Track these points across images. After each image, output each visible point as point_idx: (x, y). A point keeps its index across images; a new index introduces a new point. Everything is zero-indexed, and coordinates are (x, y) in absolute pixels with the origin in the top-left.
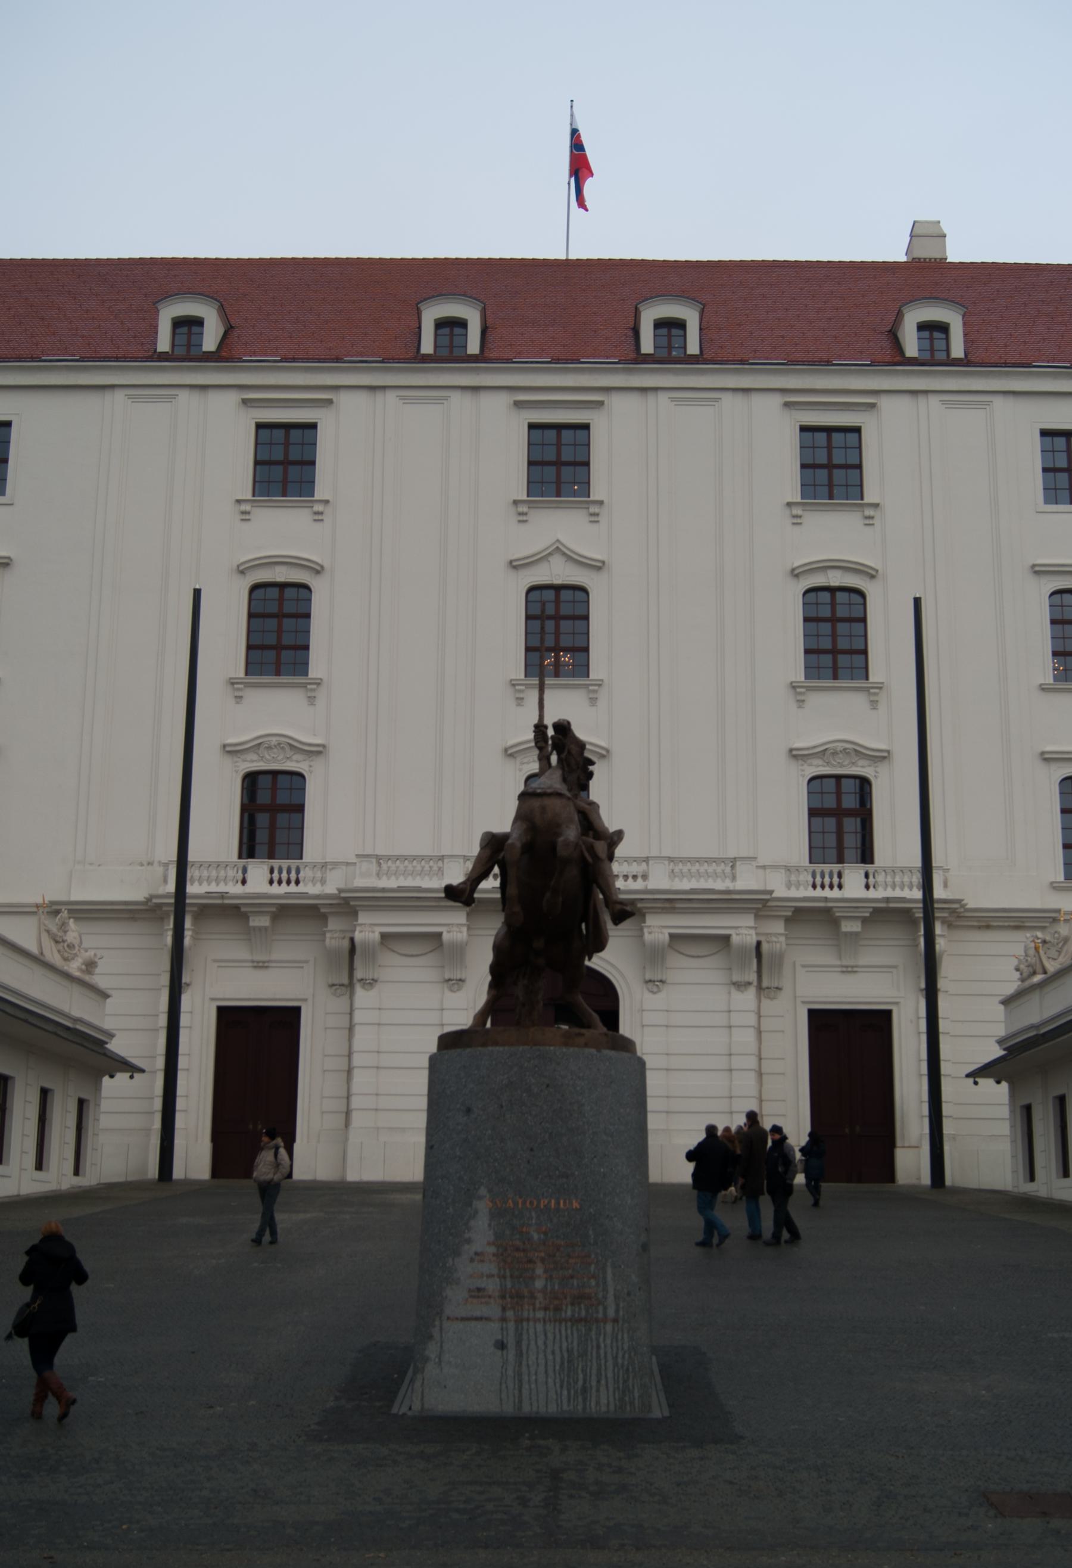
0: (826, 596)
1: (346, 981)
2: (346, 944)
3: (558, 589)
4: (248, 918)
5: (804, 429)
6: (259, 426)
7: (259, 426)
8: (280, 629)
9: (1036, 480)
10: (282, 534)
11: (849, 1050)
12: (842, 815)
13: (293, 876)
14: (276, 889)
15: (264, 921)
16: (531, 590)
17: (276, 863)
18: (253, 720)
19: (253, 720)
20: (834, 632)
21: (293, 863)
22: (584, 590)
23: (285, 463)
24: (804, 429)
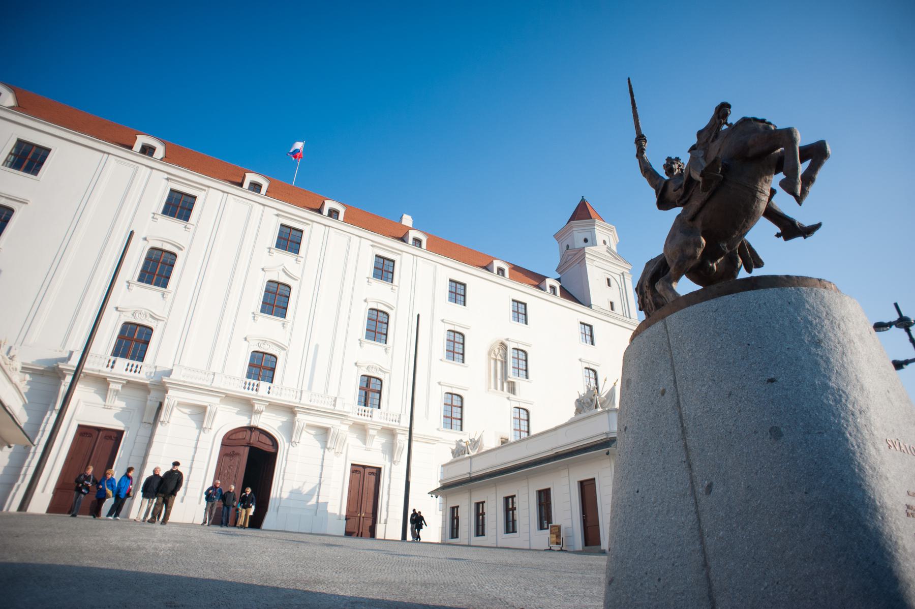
0: (375, 313)
1: (152, 422)
2: (157, 405)
3: (278, 283)
4: (109, 384)
5: (377, 256)
6: (172, 191)
7: (172, 191)
8: (158, 268)
9: (447, 294)
10: (169, 233)
11: (365, 483)
12: (370, 390)
13: (138, 369)
14: (128, 373)
15: (119, 387)
16: (269, 281)
17: (131, 362)
18: (136, 301)
19: (136, 301)
20: (377, 326)
21: (140, 364)
22: (289, 287)
23: (179, 206)
24: (377, 256)
